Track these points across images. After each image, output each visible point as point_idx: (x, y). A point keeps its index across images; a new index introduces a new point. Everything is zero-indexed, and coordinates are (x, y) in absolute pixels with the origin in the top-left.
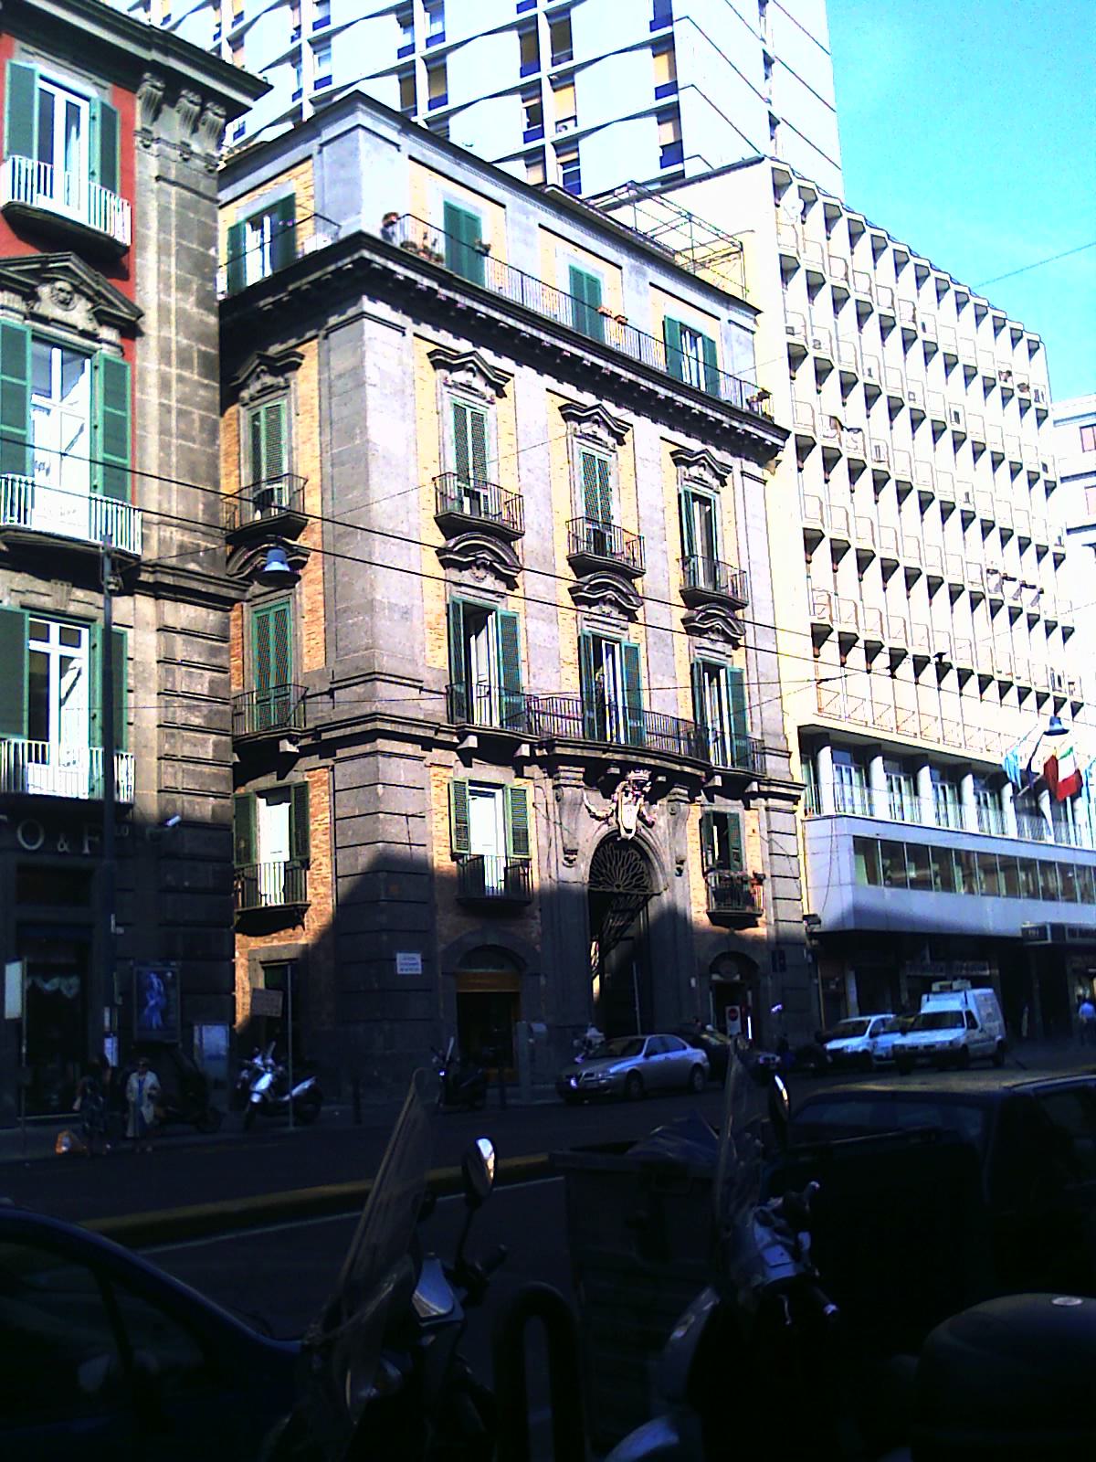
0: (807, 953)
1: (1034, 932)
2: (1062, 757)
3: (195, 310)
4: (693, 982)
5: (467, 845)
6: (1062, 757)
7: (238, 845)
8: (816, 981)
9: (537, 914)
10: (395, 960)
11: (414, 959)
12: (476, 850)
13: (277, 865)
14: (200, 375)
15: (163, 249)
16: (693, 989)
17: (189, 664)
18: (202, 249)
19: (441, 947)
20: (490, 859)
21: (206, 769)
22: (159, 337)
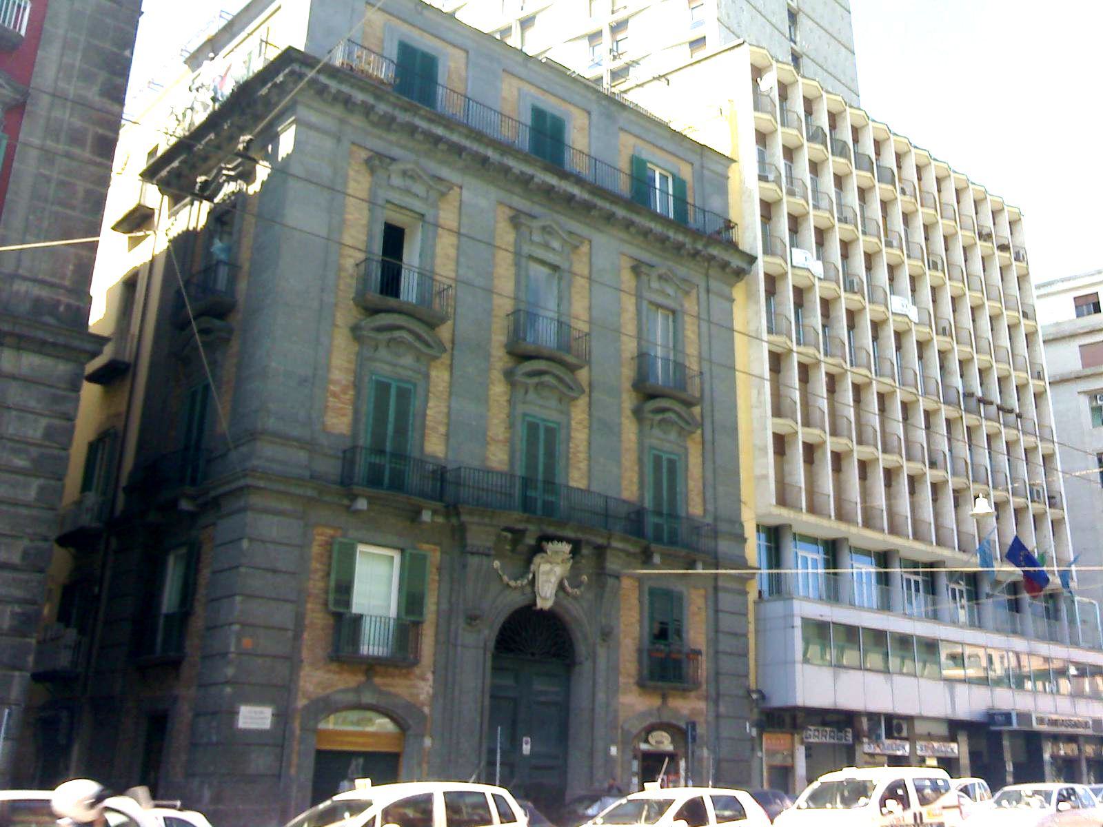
0: (751, 726)
1: (1000, 718)
2: (522, 45)
3: (97, 98)
4: (614, 750)
5: (348, 604)
6: (522, 45)
7: (100, 591)
8: (759, 754)
9: (430, 676)
10: (237, 713)
11: (261, 713)
12: (356, 608)
13: (378, 619)
14: (93, 152)
15: (67, 45)
16: (612, 757)
17: (23, 410)
18: (115, 50)
19: (301, 702)
20: (368, 619)
21: (25, 511)
22: (48, 119)
